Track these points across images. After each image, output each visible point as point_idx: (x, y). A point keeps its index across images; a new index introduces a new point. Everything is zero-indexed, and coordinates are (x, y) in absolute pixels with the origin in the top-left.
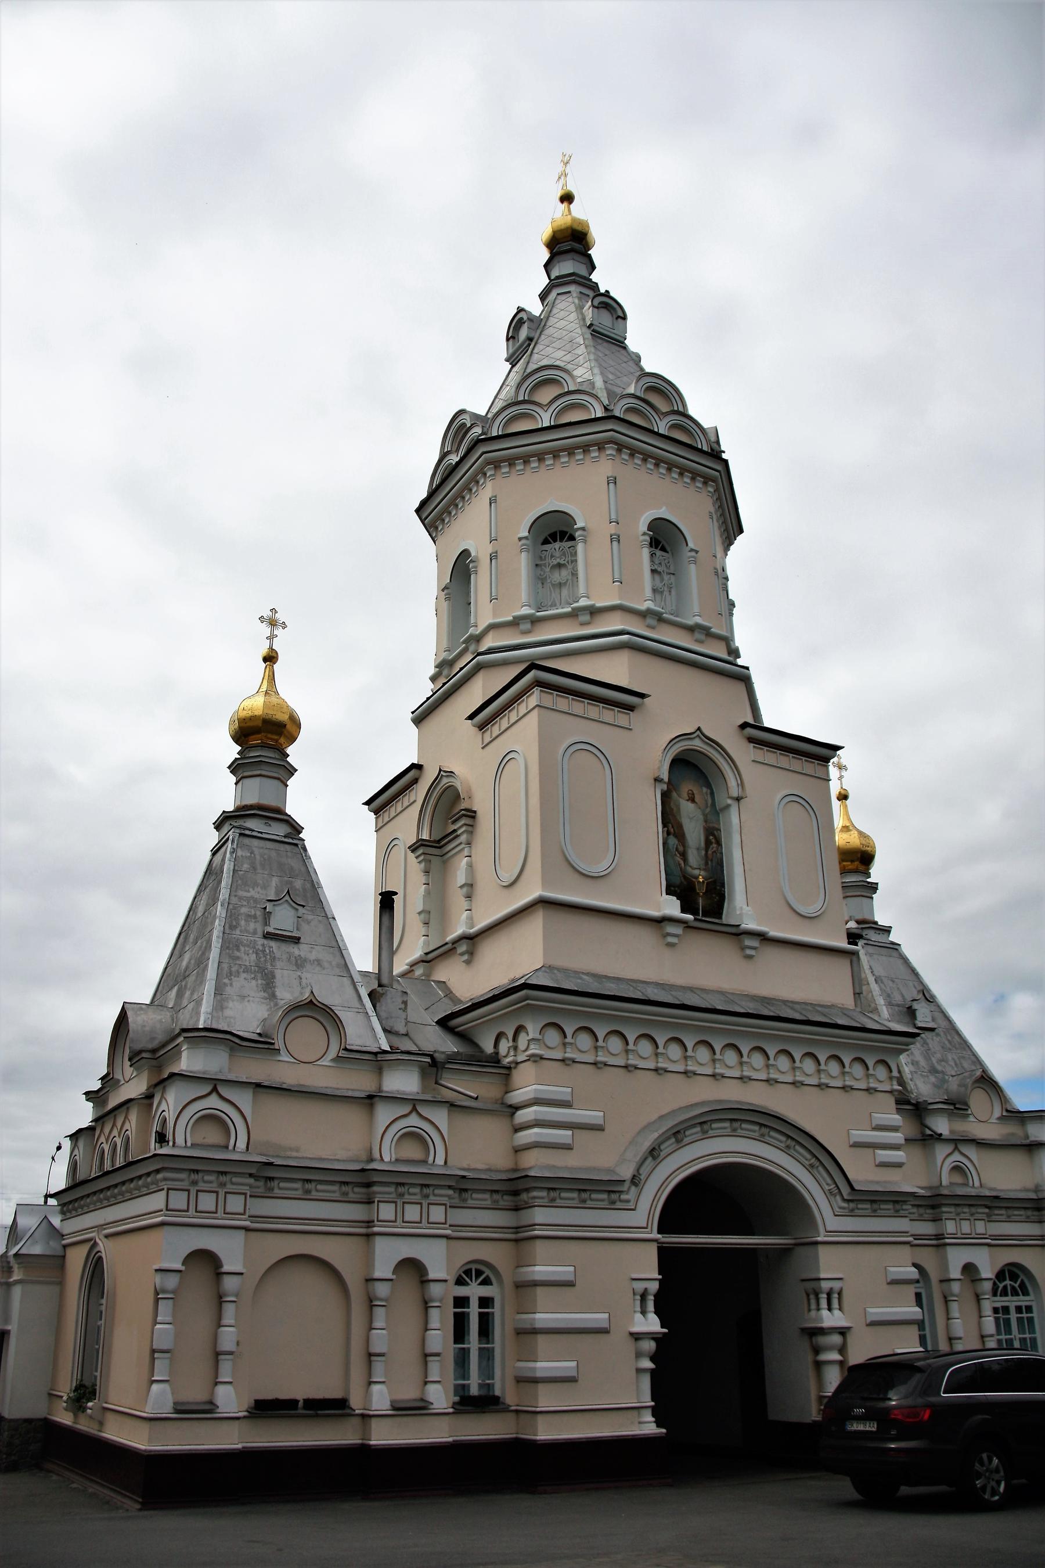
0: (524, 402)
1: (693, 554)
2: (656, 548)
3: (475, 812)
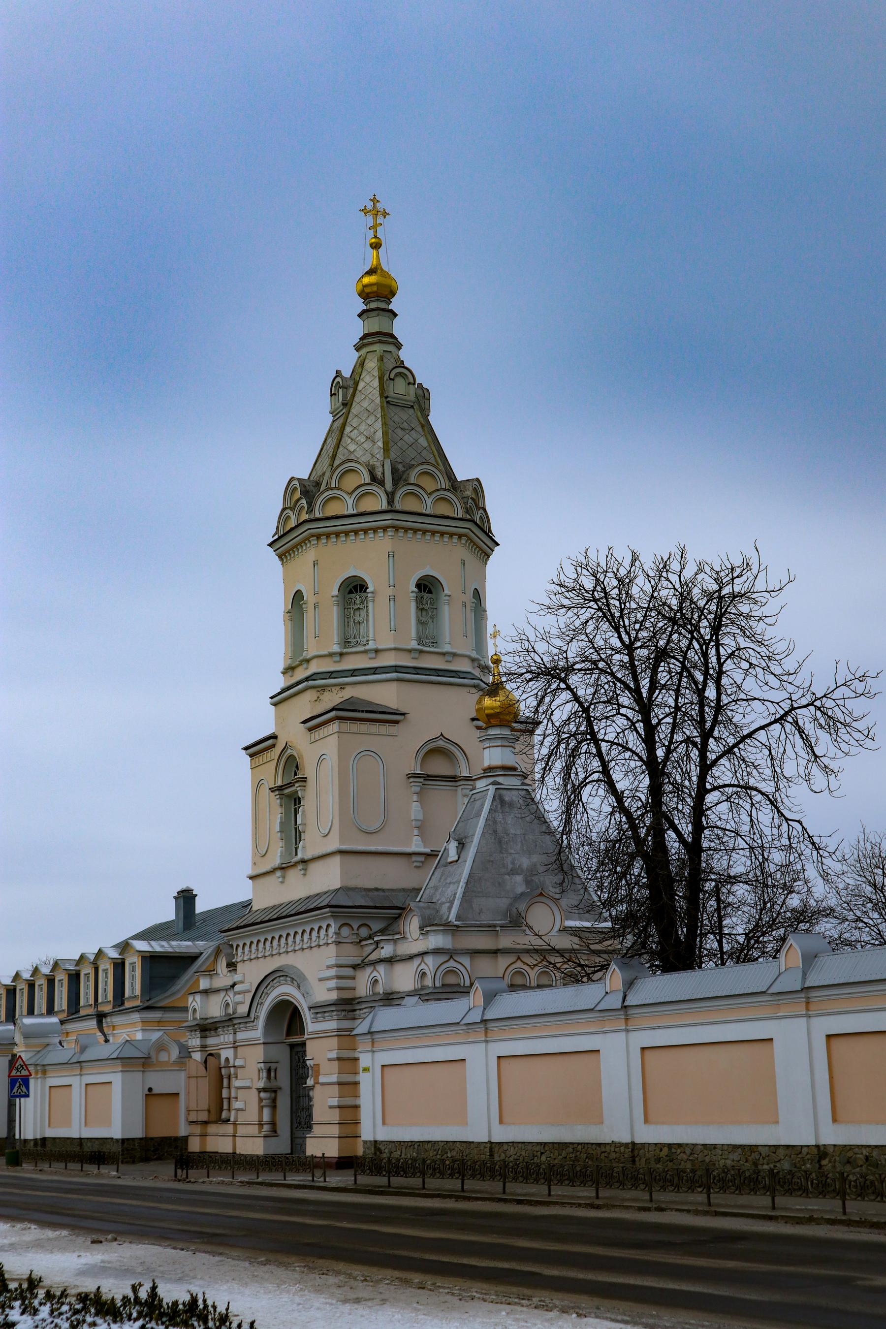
0: (335, 488)
1: (447, 598)
2: (424, 592)
3: (306, 778)
